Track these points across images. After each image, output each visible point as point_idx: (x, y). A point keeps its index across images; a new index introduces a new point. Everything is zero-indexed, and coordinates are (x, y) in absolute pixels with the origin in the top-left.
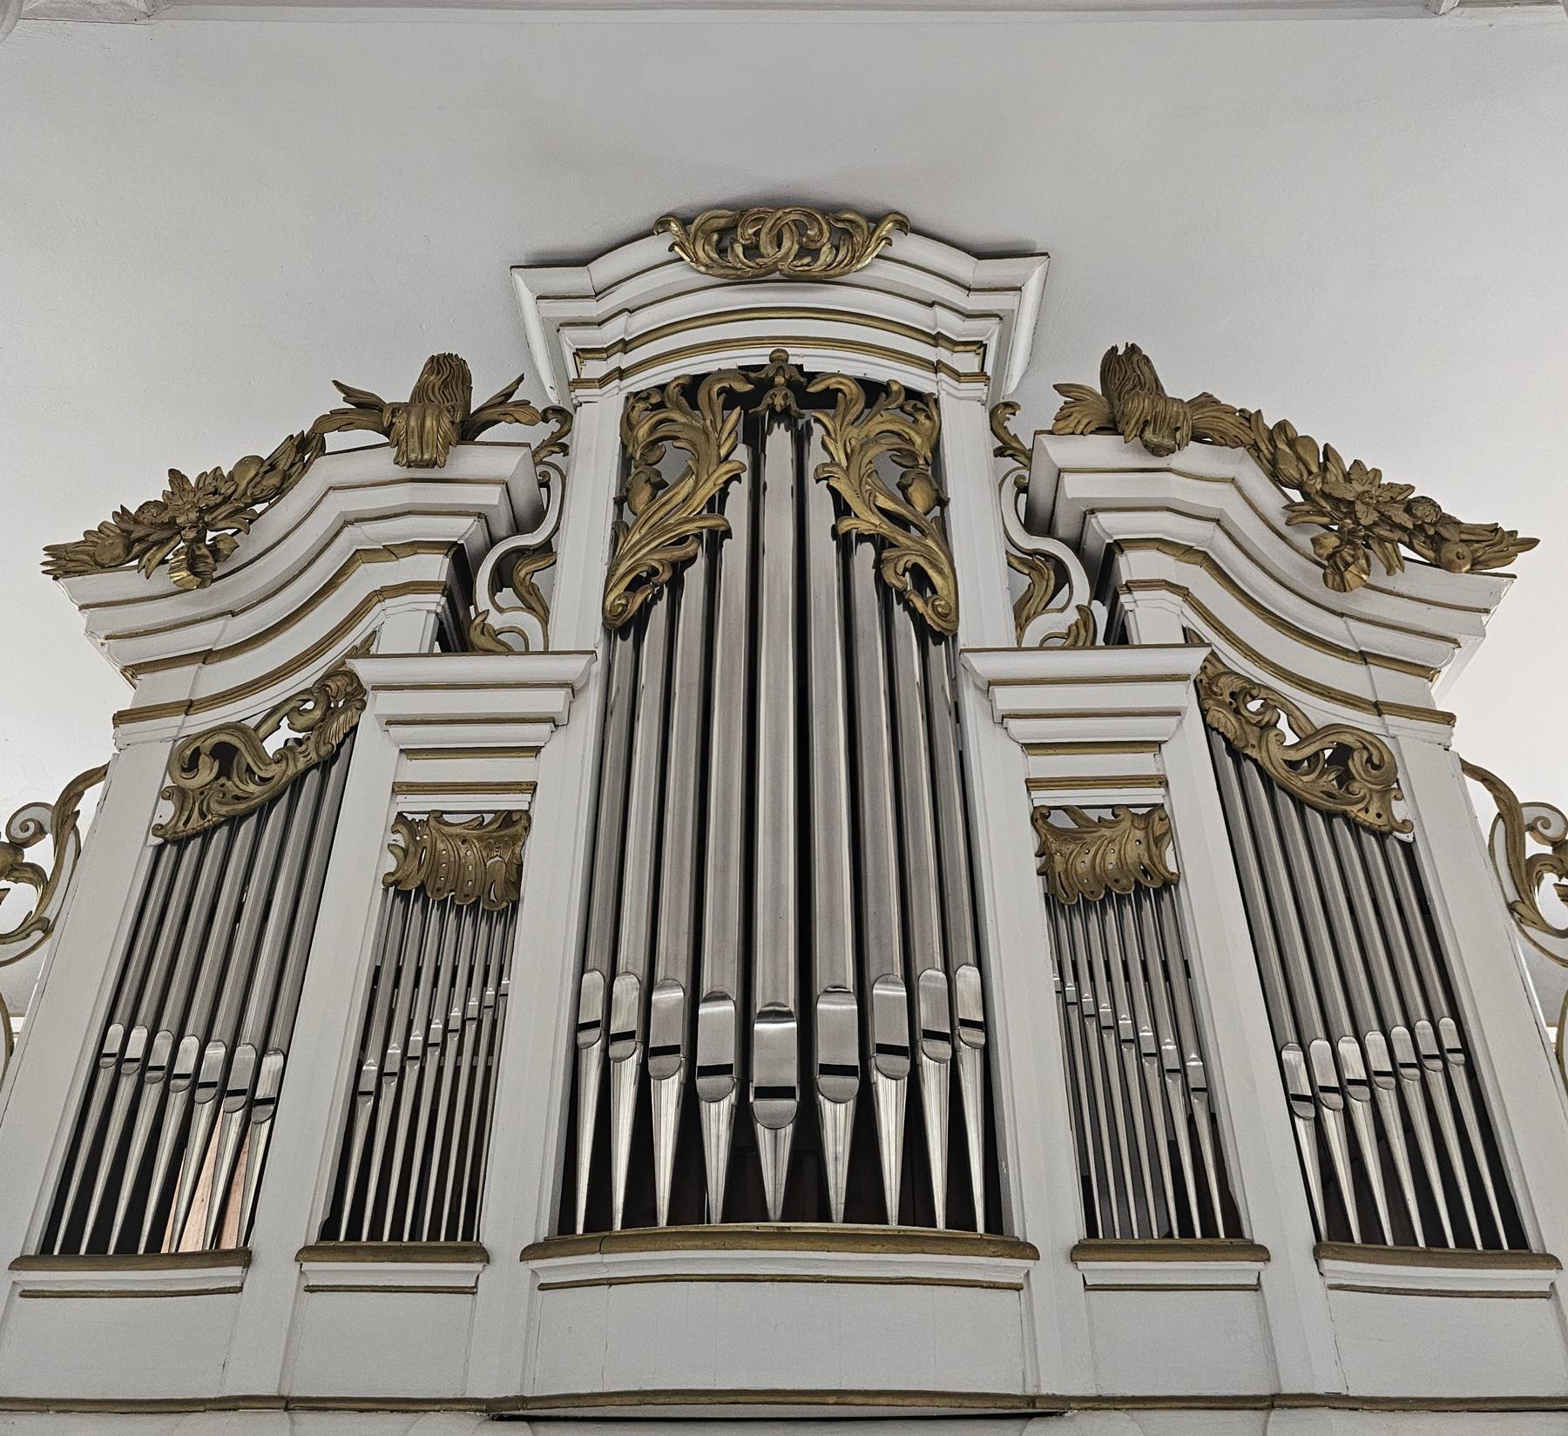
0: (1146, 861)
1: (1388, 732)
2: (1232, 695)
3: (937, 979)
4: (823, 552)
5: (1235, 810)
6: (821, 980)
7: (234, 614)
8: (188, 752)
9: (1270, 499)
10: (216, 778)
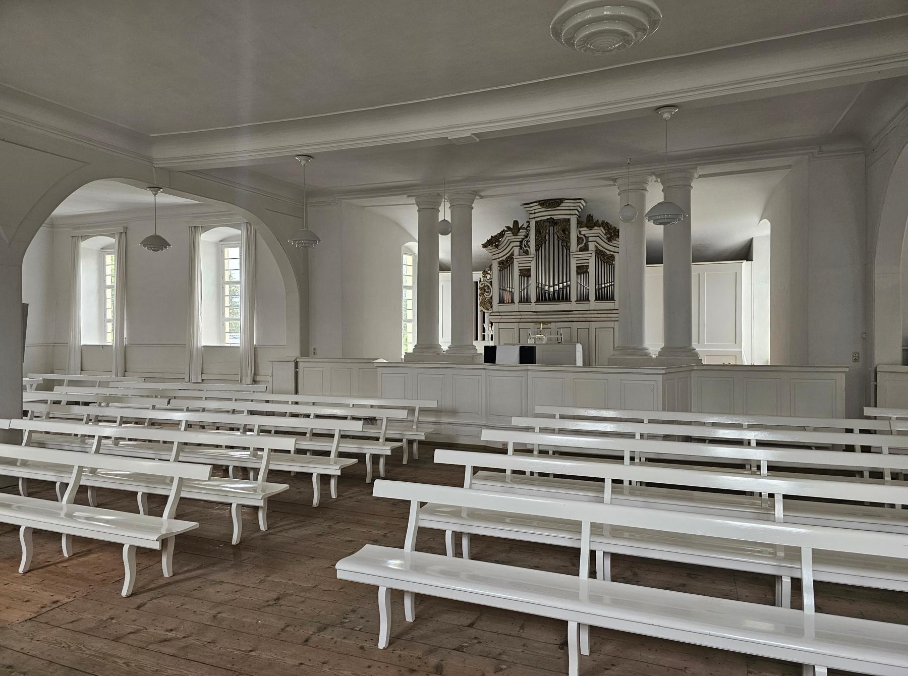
4: (556, 242)
9: (604, 232)
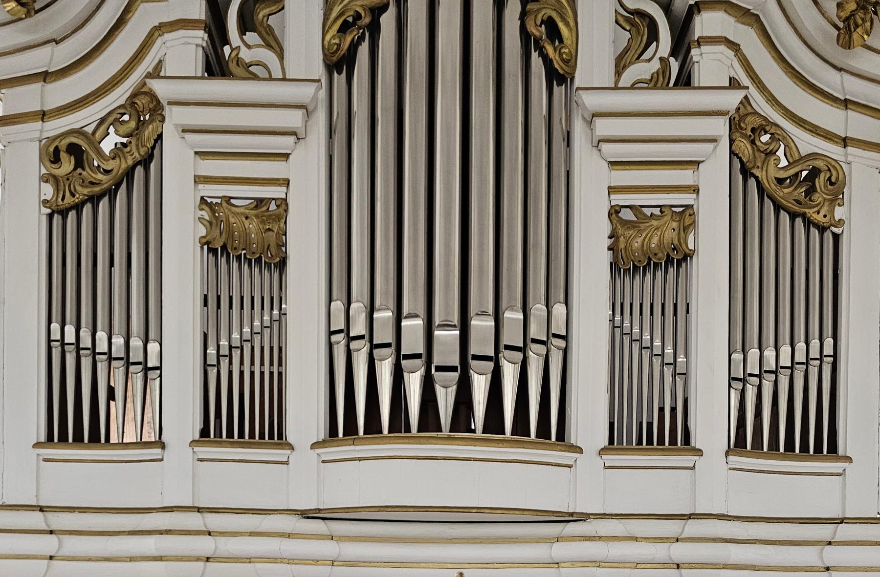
0: (676, 242)
1: (846, 160)
2: (753, 130)
3: (541, 310)
5: (737, 211)
6: (473, 307)
7: (57, 42)
8: (52, 149)
10: (75, 169)
